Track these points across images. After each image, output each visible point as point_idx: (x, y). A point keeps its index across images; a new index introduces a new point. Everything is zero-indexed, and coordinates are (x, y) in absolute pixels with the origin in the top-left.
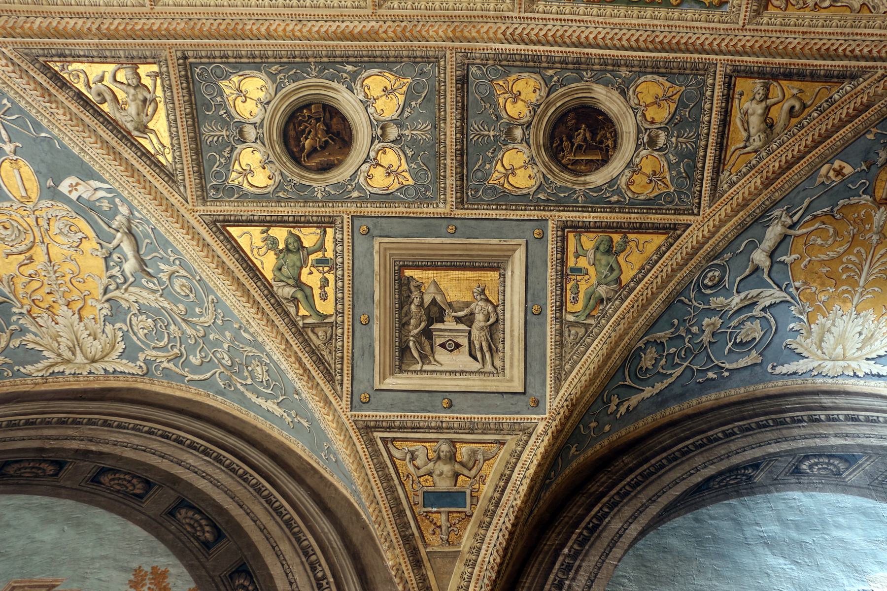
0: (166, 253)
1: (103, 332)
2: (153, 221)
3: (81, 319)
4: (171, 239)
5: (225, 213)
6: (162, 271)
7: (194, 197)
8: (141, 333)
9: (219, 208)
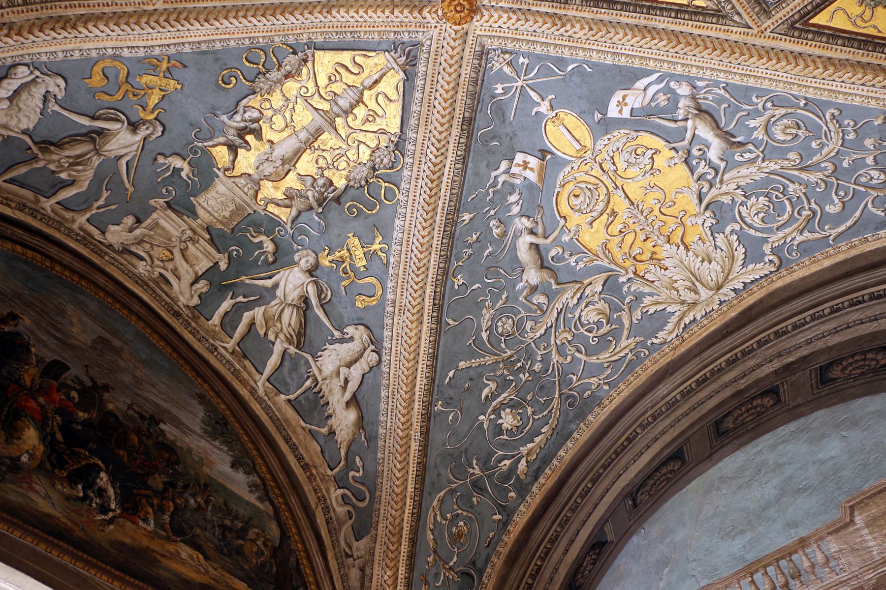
0: (751, 103)
1: (716, 247)
2: (722, 77)
3: (687, 249)
4: (751, 82)
5: (798, 9)
6: (755, 128)
7: (755, 17)
8: (757, 222)
9: (788, 9)
